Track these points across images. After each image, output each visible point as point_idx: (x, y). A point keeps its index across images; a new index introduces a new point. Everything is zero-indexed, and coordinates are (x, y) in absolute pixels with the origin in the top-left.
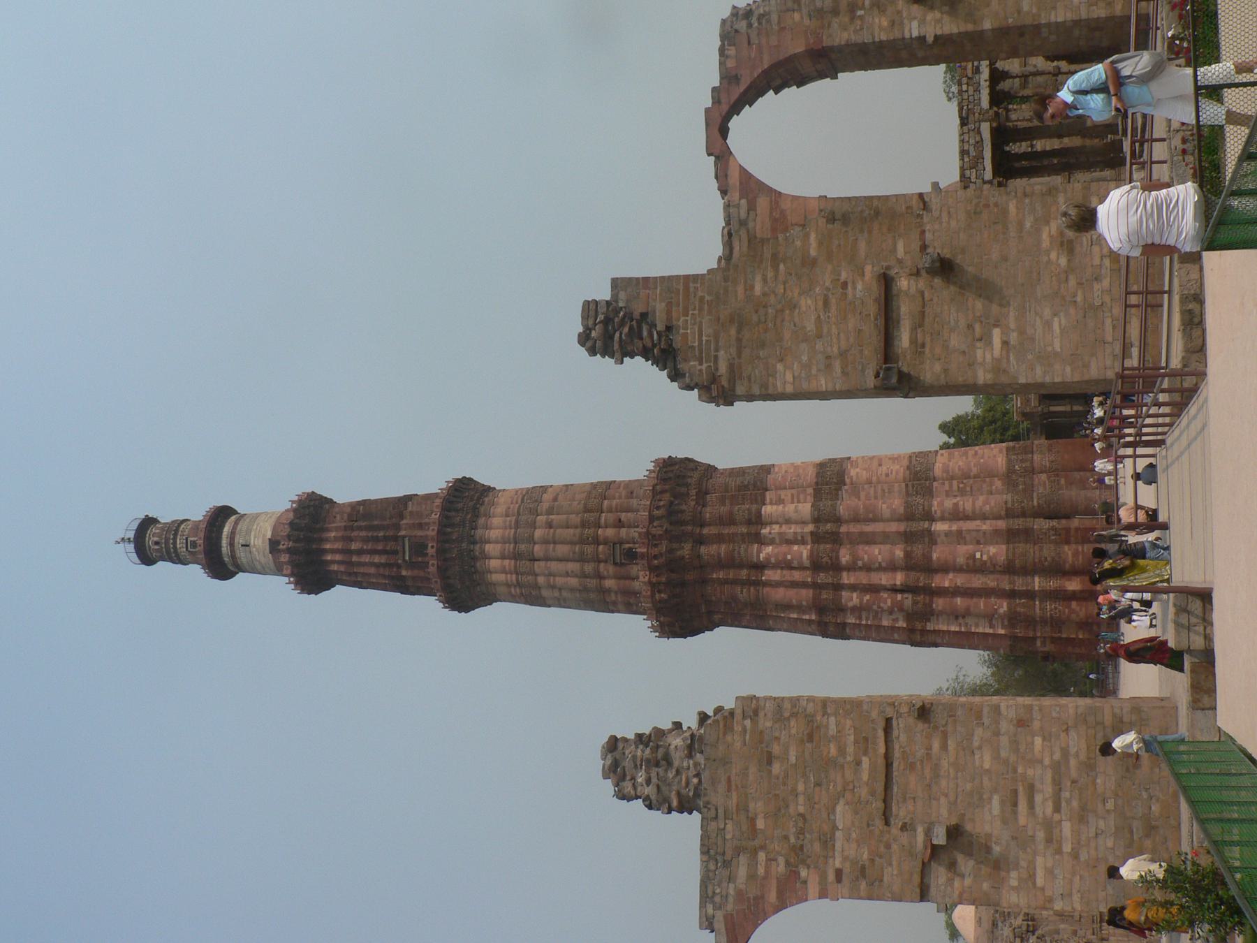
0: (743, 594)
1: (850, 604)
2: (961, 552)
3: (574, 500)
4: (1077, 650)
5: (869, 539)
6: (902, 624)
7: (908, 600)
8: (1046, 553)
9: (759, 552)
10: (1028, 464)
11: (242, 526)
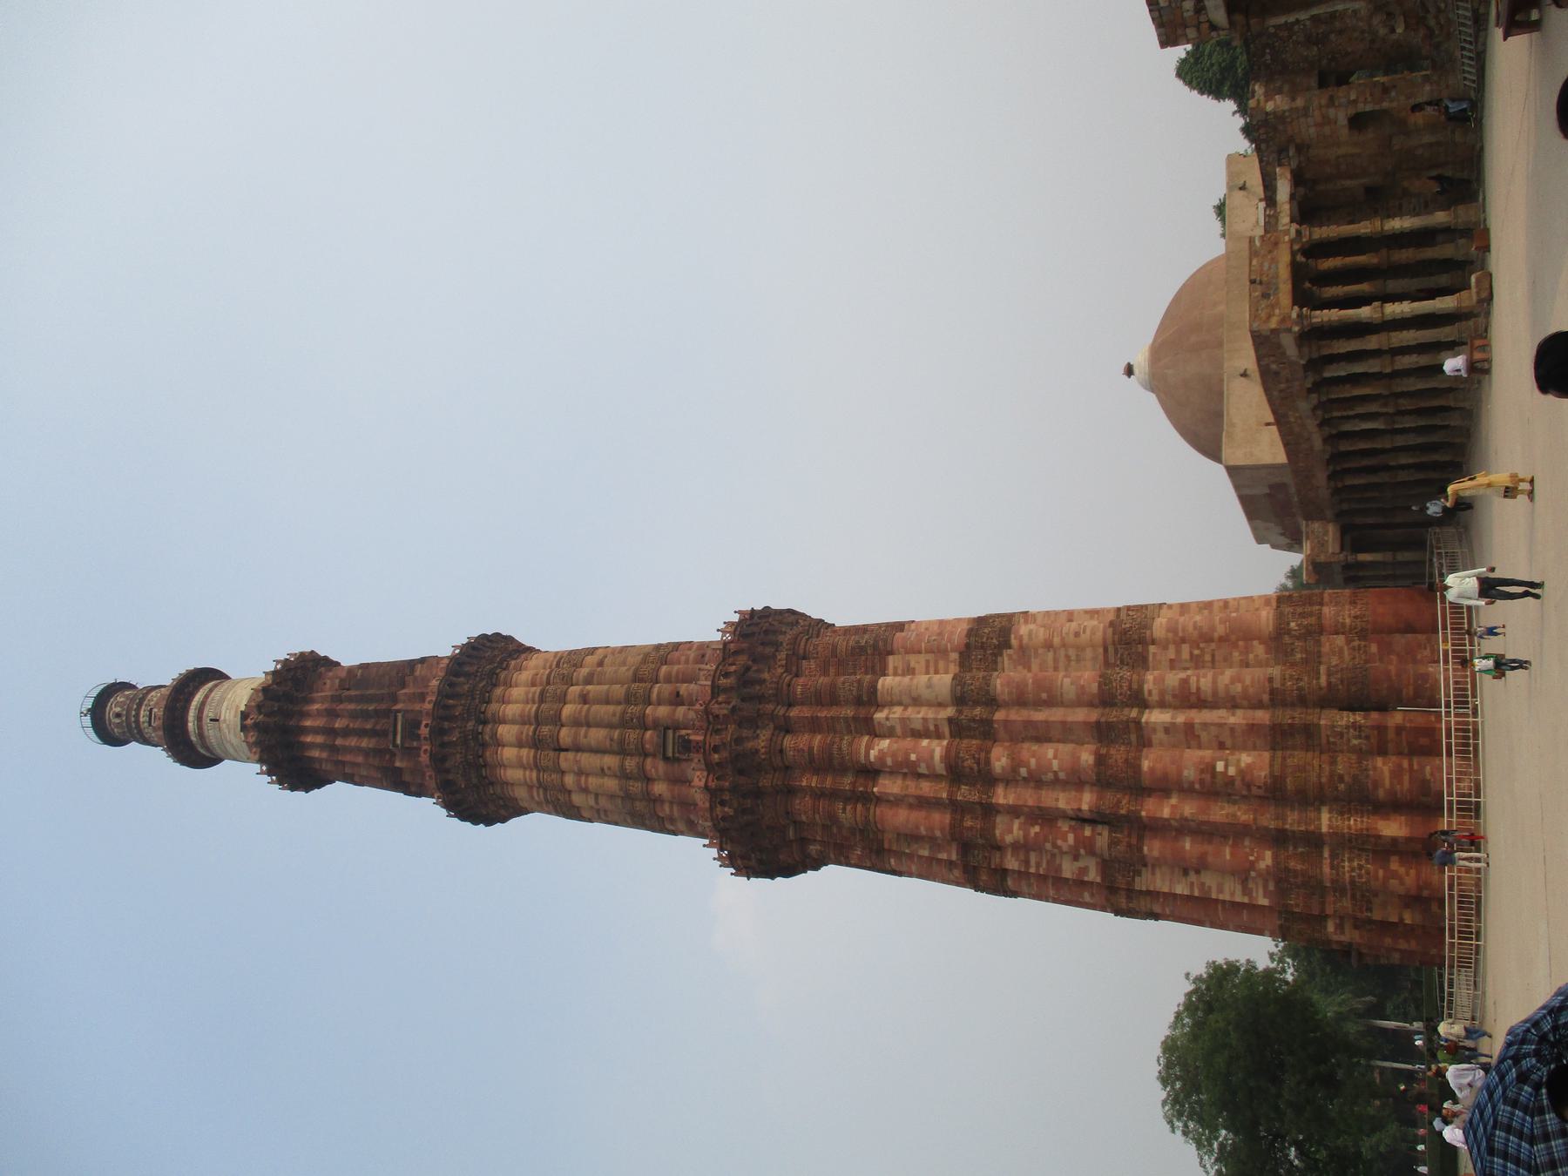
0: (847, 815)
1: (1009, 839)
2: (1190, 762)
3: (624, 663)
4: (1403, 945)
5: (1042, 735)
6: (1093, 875)
7: (1102, 838)
8: (1340, 769)
9: (869, 747)
10: (1312, 620)
11: (216, 694)
